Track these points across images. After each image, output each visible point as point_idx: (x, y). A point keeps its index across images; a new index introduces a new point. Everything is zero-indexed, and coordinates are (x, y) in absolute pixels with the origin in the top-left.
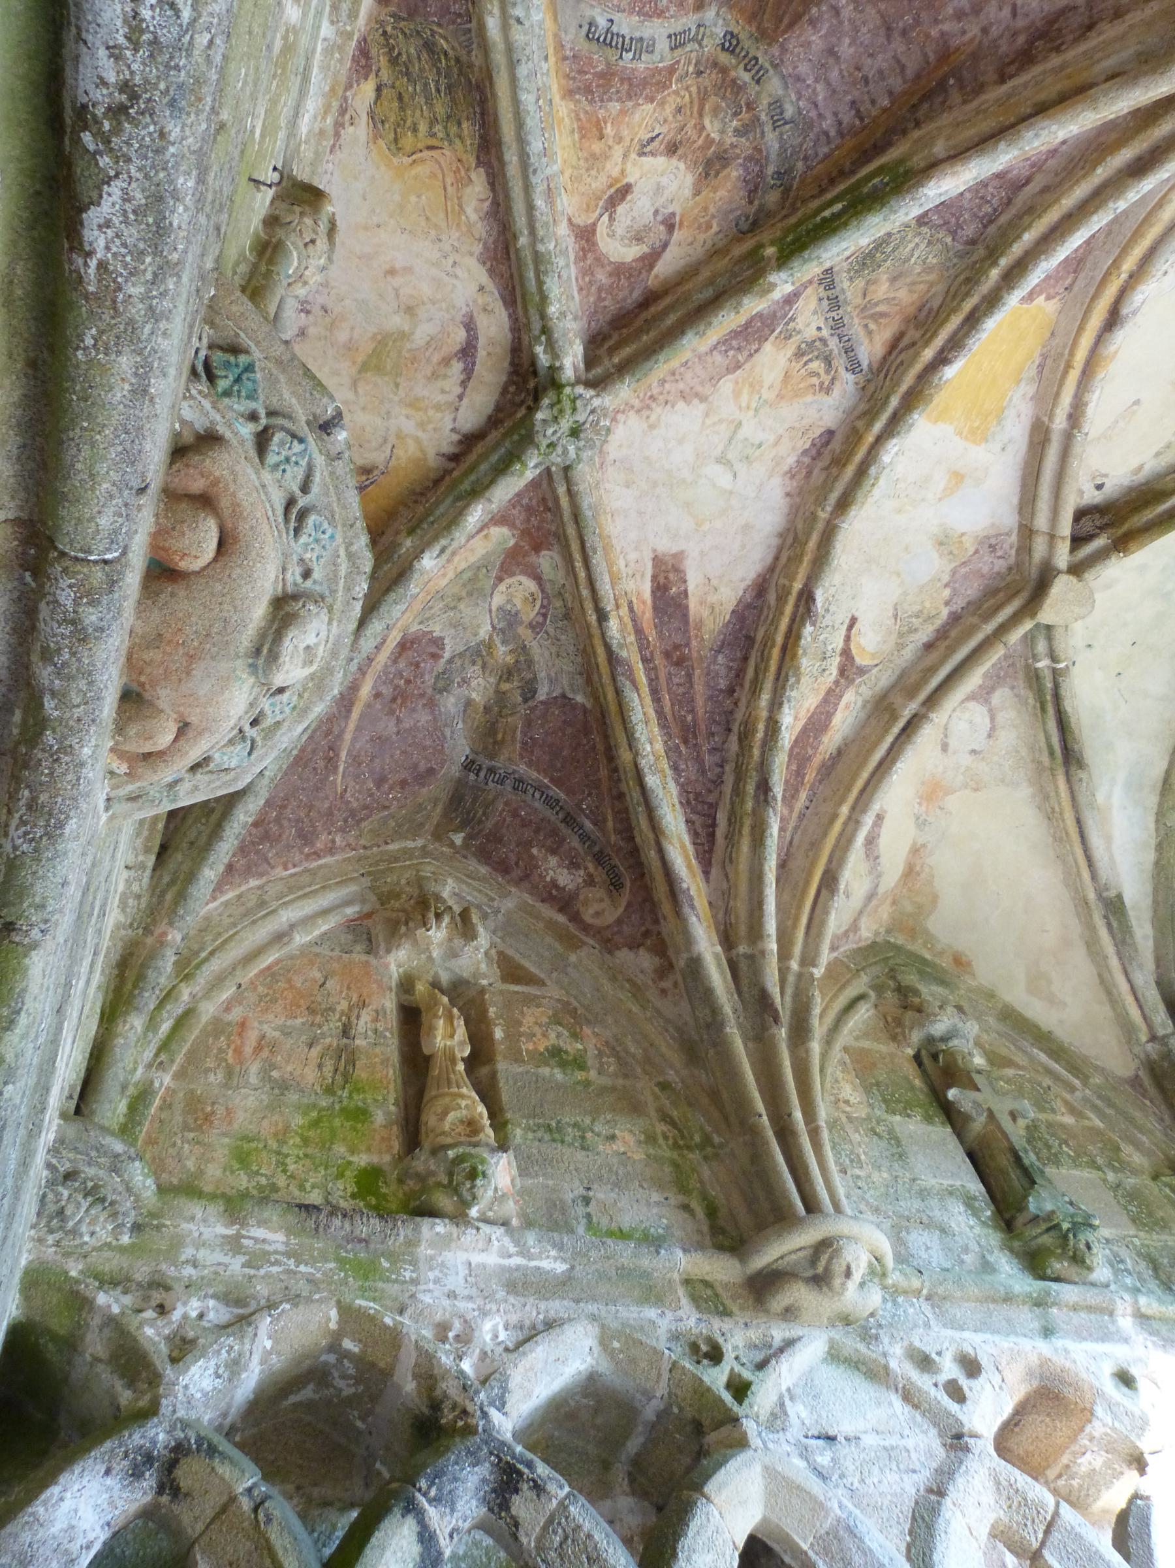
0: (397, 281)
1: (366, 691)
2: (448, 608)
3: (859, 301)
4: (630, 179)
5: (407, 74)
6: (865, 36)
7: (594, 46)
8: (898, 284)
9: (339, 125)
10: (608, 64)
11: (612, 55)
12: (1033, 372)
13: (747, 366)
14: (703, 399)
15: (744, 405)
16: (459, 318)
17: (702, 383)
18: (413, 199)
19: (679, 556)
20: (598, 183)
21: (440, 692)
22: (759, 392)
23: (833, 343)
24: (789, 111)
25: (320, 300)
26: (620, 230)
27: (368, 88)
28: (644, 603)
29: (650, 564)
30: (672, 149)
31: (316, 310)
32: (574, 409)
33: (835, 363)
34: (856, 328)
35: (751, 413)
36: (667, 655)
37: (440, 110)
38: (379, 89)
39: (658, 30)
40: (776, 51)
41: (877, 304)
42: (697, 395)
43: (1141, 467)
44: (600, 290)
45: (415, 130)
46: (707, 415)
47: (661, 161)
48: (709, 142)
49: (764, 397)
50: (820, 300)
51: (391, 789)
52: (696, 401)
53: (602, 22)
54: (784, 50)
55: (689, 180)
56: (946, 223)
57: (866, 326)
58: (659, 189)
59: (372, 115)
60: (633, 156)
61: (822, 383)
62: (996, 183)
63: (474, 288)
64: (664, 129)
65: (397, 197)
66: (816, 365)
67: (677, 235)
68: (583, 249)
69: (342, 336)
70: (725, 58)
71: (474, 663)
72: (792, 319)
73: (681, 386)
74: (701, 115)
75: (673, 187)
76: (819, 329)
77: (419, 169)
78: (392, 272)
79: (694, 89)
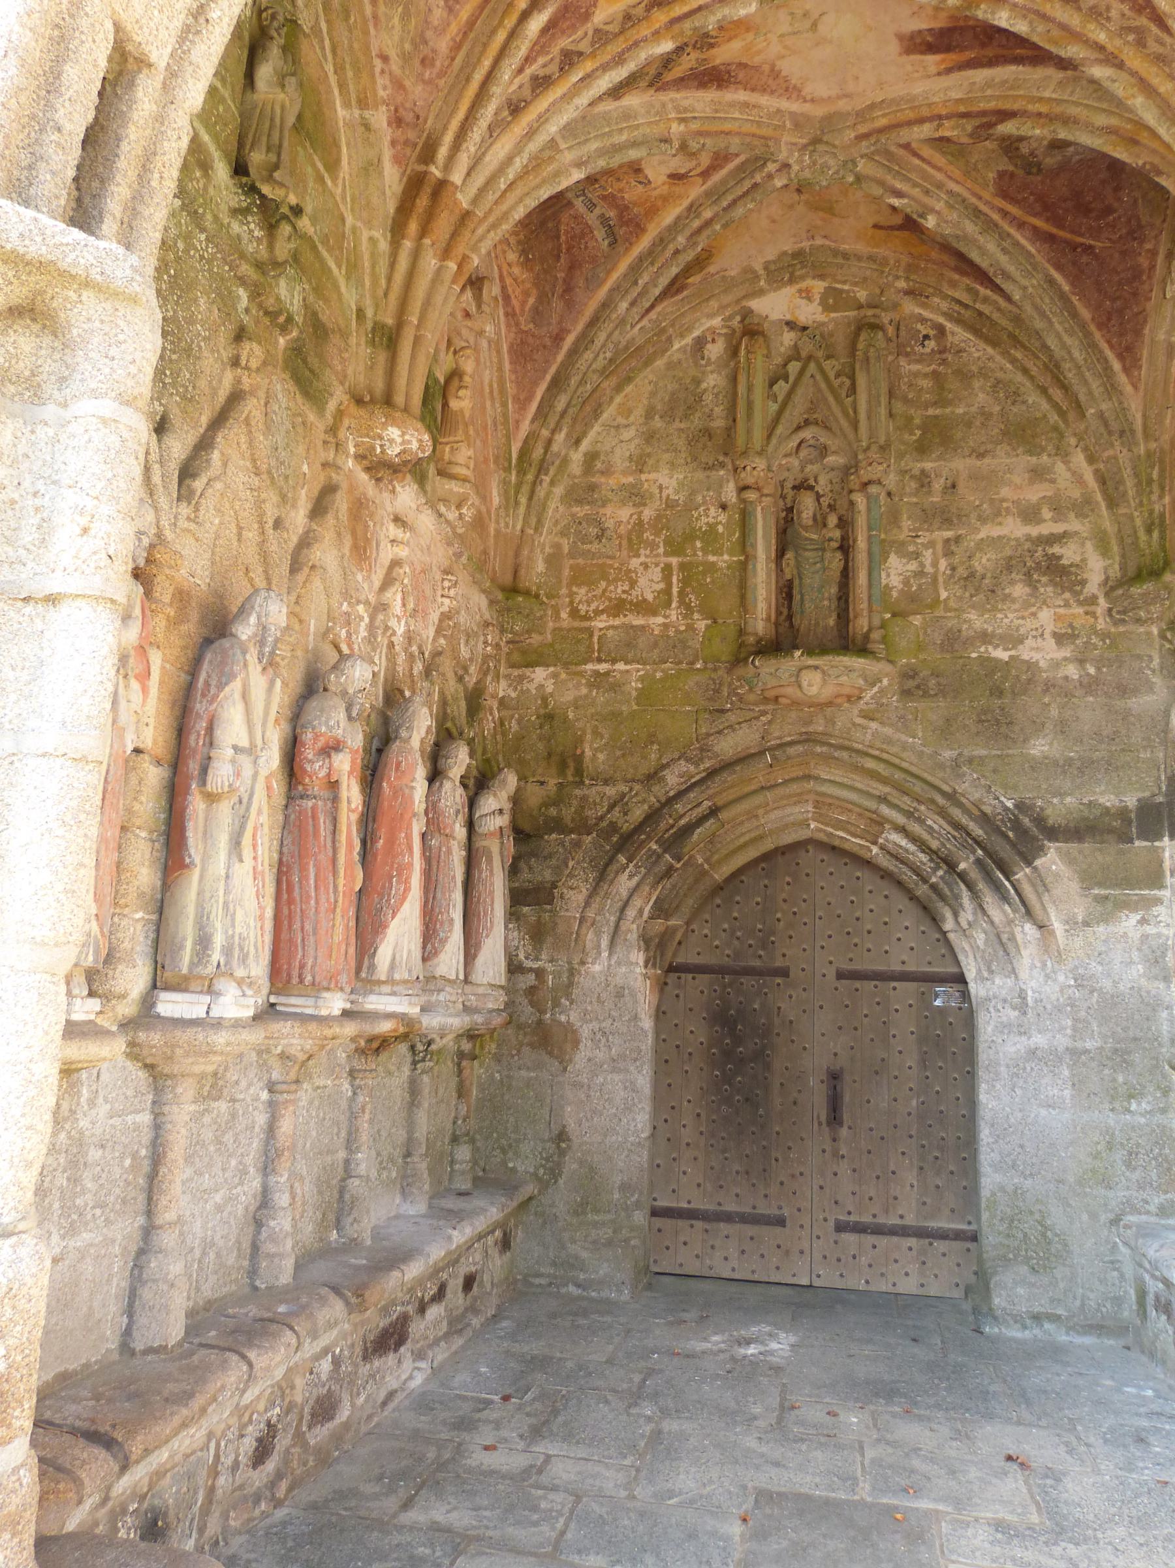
1: (1038, 223)
2: (975, 169)
11: (616, 229)
14: (773, 67)
19: (900, 37)
21: (1040, 170)
26: (694, 163)
27: (690, 280)
28: (943, 61)
29: (913, 57)
36: (983, 45)
39: (592, 218)
46: (783, 57)
51: (1119, 199)
58: (660, 163)
69: (819, 223)
71: (1017, 149)
78: (774, 221)
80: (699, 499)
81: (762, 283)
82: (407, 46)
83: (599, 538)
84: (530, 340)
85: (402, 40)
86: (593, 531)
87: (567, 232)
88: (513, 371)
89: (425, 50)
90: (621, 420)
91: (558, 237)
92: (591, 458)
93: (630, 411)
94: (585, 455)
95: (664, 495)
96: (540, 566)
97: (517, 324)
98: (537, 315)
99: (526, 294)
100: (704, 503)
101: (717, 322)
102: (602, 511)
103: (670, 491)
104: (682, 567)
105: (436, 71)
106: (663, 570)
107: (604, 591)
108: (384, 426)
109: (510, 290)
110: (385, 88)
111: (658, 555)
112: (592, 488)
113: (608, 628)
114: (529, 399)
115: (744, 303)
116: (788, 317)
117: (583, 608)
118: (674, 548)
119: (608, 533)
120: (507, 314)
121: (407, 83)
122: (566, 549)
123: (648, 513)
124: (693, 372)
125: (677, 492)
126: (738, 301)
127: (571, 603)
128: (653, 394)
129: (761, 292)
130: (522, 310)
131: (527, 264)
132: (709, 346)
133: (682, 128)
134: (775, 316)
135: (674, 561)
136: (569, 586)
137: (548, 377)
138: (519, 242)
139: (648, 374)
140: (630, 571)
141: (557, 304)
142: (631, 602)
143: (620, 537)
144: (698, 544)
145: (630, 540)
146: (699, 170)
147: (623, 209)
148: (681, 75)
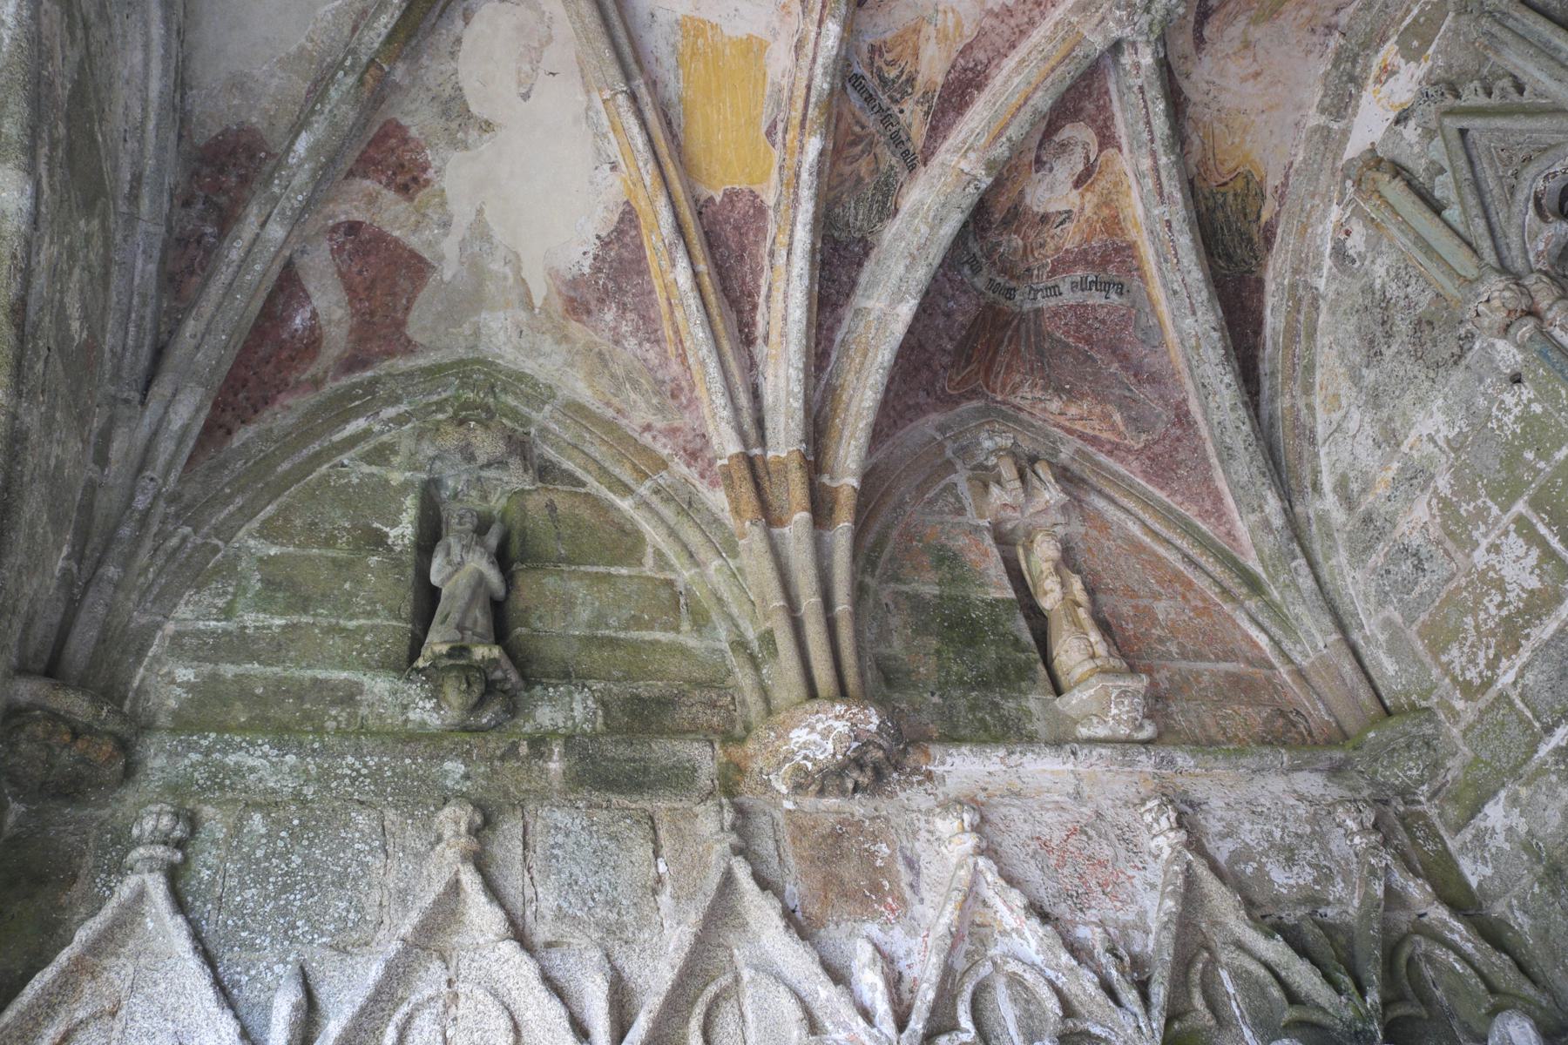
0: (1255, 68)
3: (878, 150)
4: (1075, 192)
5: (1241, 234)
6: (932, 335)
7: (1117, 280)
8: (854, 177)
9: (1285, 185)
10: (1105, 270)
11: (1103, 277)
12: (671, 112)
13: (954, 55)
14: (990, 13)
15: (950, 15)
16: (1208, 46)
17: (993, 28)
18: (1237, 140)
20: (1102, 184)
22: (938, 31)
23: (884, 100)
24: (966, 270)
25: (1315, 39)
26: (1079, 149)
30: (1045, 219)
31: (1320, 30)
32: (1151, 25)
33: (876, 81)
34: (871, 121)
35: (941, 8)
37: (1220, 215)
38: (1259, 217)
39: (1069, 297)
40: (982, 302)
41: (863, 152)
42: (997, 16)
43: (467, 19)
44: (1090, 94)
45: (1235, 195)
47: (1052, 209)
48: (1017, 232)
49: (932, 27)
50: (909, 139)
52: (996, 9)
53: (1114, 296)
54: (978, 305)
55: (1028, 200)
56: (846, 248)
57: (863, 127)
58: (1051, 188)
59: (1263, 197)
60: (1076, 210)
61: (881, 55)
62: (834, 298)
63: (1194, 77)
64: (1053, 231)
65: (1248, 138)
66: (892, 73)
67: (1033, 156)
68: (1108, 128)
69: (1306, 12)
70: (1013, 284)
72: (927, 113)
73: (1013, 22)
74: (1025, 246)
75: (1040, 191)
76: (902, 111)
77: (1232, 165)
78: (1257, 75)
79: (1031, 259)
80: (1481, 402)
81: (1335, 126)
82: (655, 401)
83: (1419, 567)
84: (1158, 449)
85: (648, 402)
86: (1407, 567)
87: (1067, 333)
88: (1172, 494)
89: (667, 388)
90: (1336, 416)
91: (1067, 345)
92: (1342, 486)
93: (1336, 396)
94: (1335, 490)
95: (1441, 443)
96: (1390, 667)
97: (1129, 450)
98: (1137, 423)
99: (1106, 417)
100: (1491, 402)
101: (1335, 213)
102: (1396, 534)
103: (1444, 430)
104: (1535, 504)
105: (686, 390)
106: (1518, 532)
107: (1477, 627)
108: (787, 740)
109: (1088, 431)
110: (665, 446)
111: (1497, 520)
112: (1368, 519)
113: (1521, 675)
114: (1218, 499)
115: (1340, 164)
116: (1392, 115)
117: (1472, 674)
118: (1506, 492)
119: (1423, 552)
120: (1110, 453)
121: (677, 424)
122: (1397, 617)
123: (1443, 483)
124: (1356, 287)
125: (1451, 424)
126: (1333, 174)
127: (1454, 679)
128: (1342, 355)
129: (1346, 133)
130: (1120, 433)
131: (1073, 396)
132: (1349, 243)
133: (972, 156)
134: (1377, 136)
135: (1520, 507)
136: (1436, 657)
137: (1214, 461)
138: (1045, 388)
139: (1323, 340)
140: (1483, 573)
141: (1146, 393)
142: (1519, 612)
143: (1439, 543)
144: (1529, 455)
145: (1451, 534)
146: (1094, 148)
147: (1083, 257)
148: (924, 131)
